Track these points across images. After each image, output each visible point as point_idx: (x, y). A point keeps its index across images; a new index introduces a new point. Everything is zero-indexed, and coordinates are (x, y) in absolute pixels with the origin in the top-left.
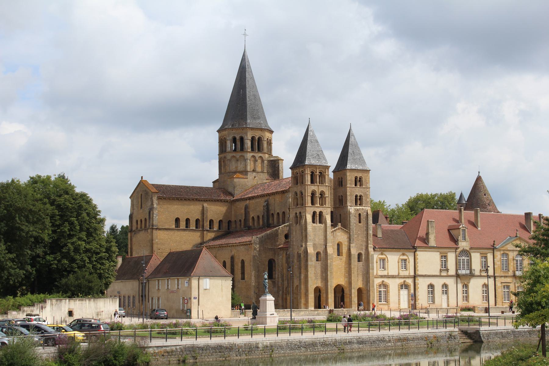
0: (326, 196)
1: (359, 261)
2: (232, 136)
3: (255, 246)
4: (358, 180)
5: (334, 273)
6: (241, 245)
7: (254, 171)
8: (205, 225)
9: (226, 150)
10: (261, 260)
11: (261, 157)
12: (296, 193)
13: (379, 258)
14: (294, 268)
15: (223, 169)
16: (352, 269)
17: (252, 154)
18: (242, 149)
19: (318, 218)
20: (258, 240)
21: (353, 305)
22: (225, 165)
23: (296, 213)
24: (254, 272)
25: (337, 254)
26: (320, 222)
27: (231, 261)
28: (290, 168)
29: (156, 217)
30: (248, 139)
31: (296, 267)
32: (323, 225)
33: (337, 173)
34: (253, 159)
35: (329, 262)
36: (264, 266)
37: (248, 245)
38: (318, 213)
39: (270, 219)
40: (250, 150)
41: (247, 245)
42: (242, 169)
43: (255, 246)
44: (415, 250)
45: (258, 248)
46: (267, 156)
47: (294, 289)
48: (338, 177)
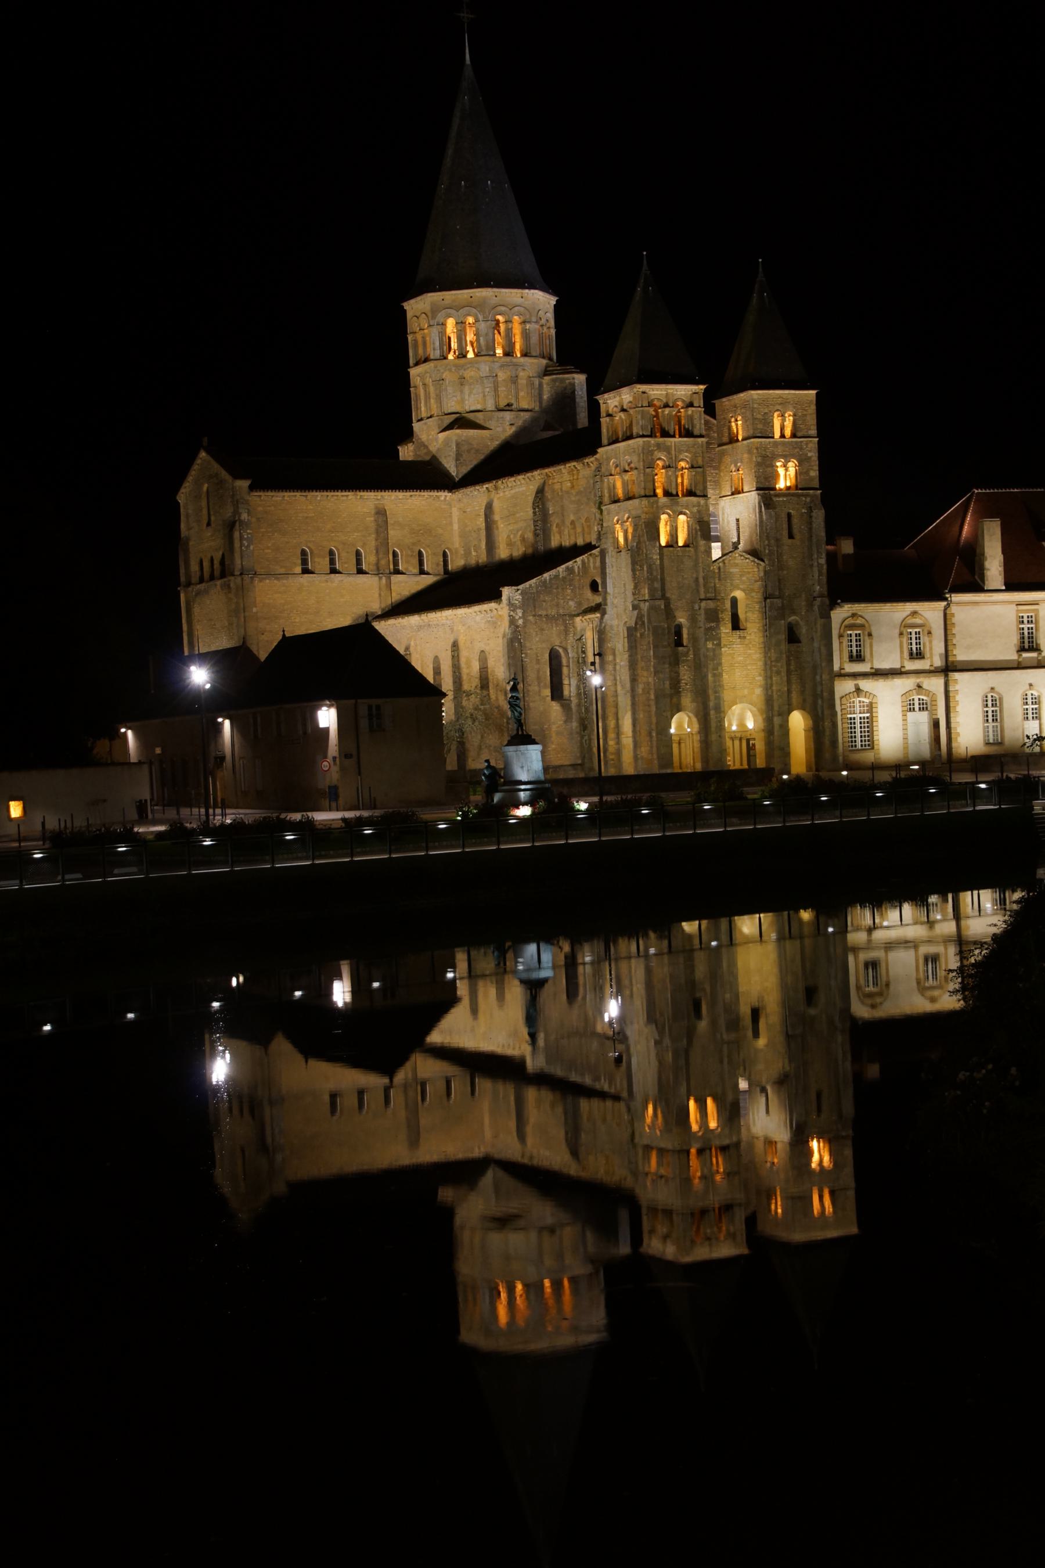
3: (512, 613)
8: (383, 562)
14: (618, 667)
15: (423, 409)
25: (730, 625)
27: (453, 656)
29: (248, 546)
31: (622, 663)
43: (512, 613)
44: (945, 603)
45: (520, 618)
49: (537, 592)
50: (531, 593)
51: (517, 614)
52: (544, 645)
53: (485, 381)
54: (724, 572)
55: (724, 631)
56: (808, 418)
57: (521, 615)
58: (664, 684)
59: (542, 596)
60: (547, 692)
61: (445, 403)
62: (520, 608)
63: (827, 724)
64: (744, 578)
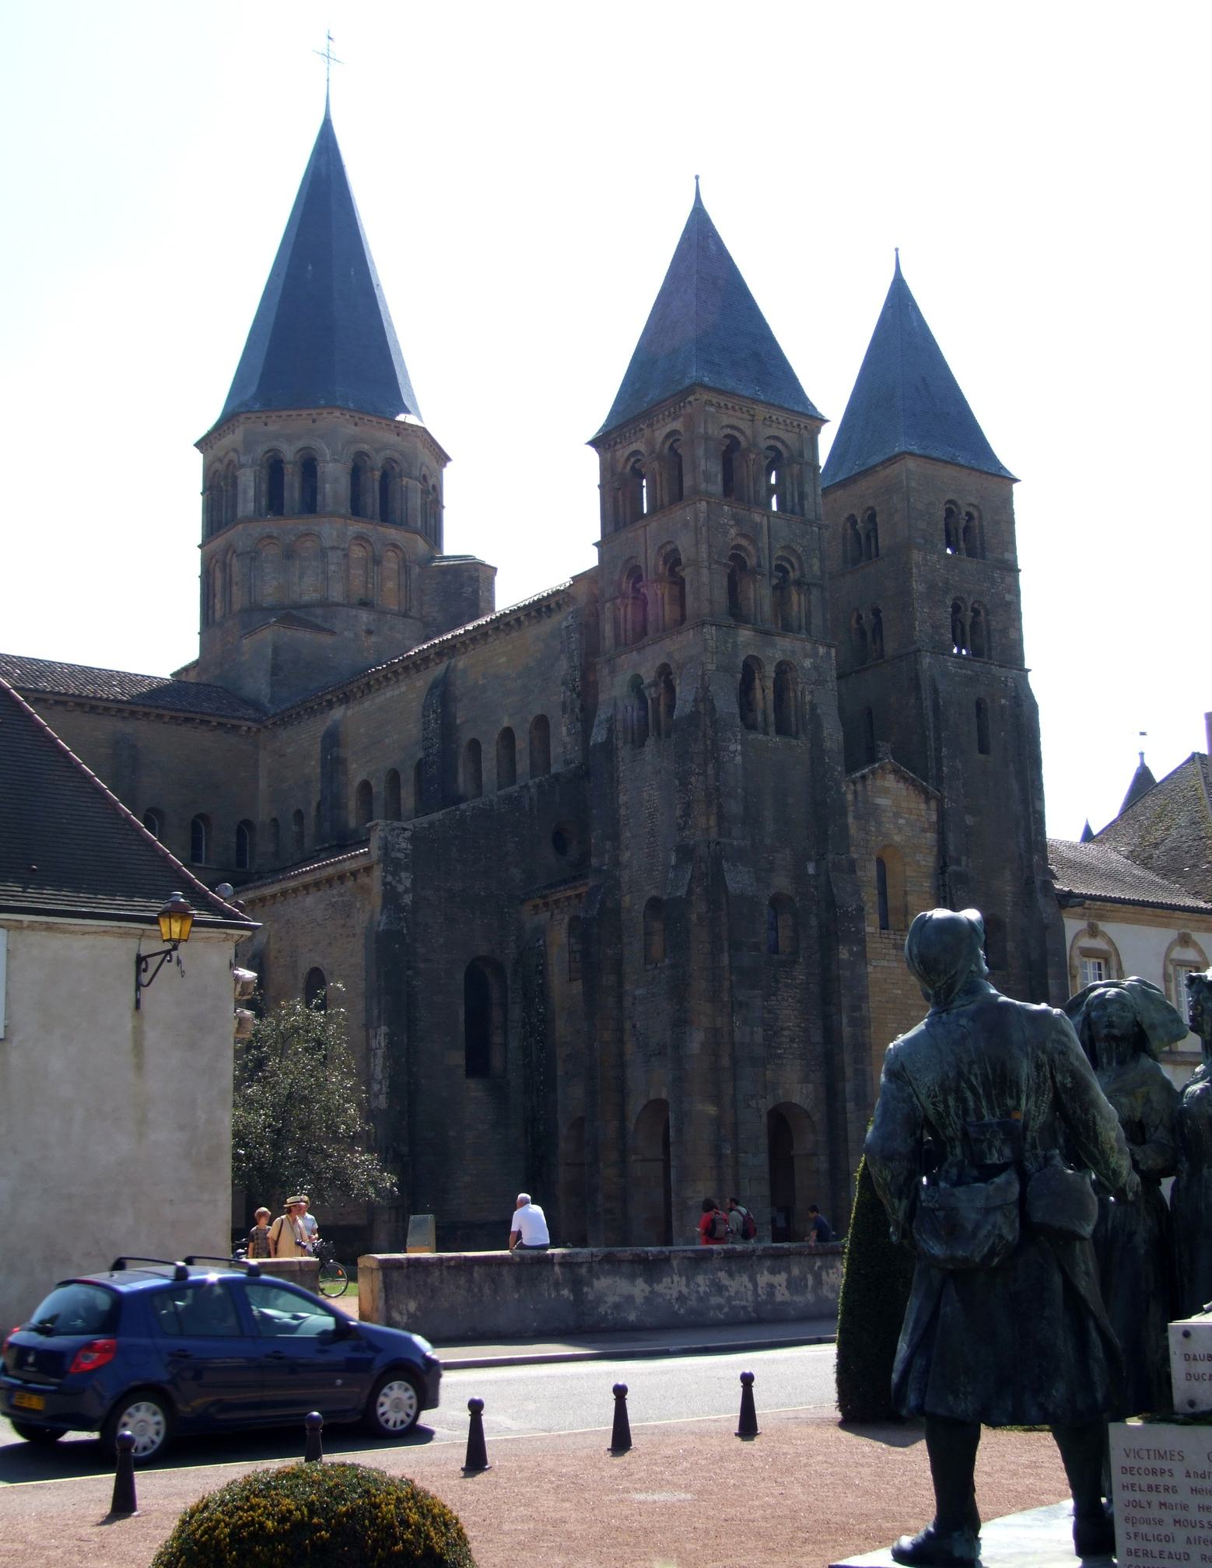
2: (265, 447)
3: (389, 878)
4: (963, 523)
6: (306, 887)
7: (364, 604)
9: (235, 514)
11: (395, 546)
12: (635, 574)
15: (218, 607)
17: (356, 527)
18: (310, 505)
19: (770, 695)
22: (228, 584)
23: (636, 684)
24: (384, 1029)
26: (782, 729)
28: (593, 443)
30: (336, 461)
32: (801, 744)
33: (840, 492)
34: (357, 552)
35: (844, 954)
37: (350, 883)
38: (770, 671)
39: (461, 770)
40: (345, 509)
41: (342, 878)
42: (306, 598)
43: (389, 878)
45: (406, 891)
46: (421, 546)
47: (631, 1126)
48: (846, 515)
51: (400, 881)
53: (330, 553)
57: (408, 885)
60: (458, 1058)
64: (901, 821)
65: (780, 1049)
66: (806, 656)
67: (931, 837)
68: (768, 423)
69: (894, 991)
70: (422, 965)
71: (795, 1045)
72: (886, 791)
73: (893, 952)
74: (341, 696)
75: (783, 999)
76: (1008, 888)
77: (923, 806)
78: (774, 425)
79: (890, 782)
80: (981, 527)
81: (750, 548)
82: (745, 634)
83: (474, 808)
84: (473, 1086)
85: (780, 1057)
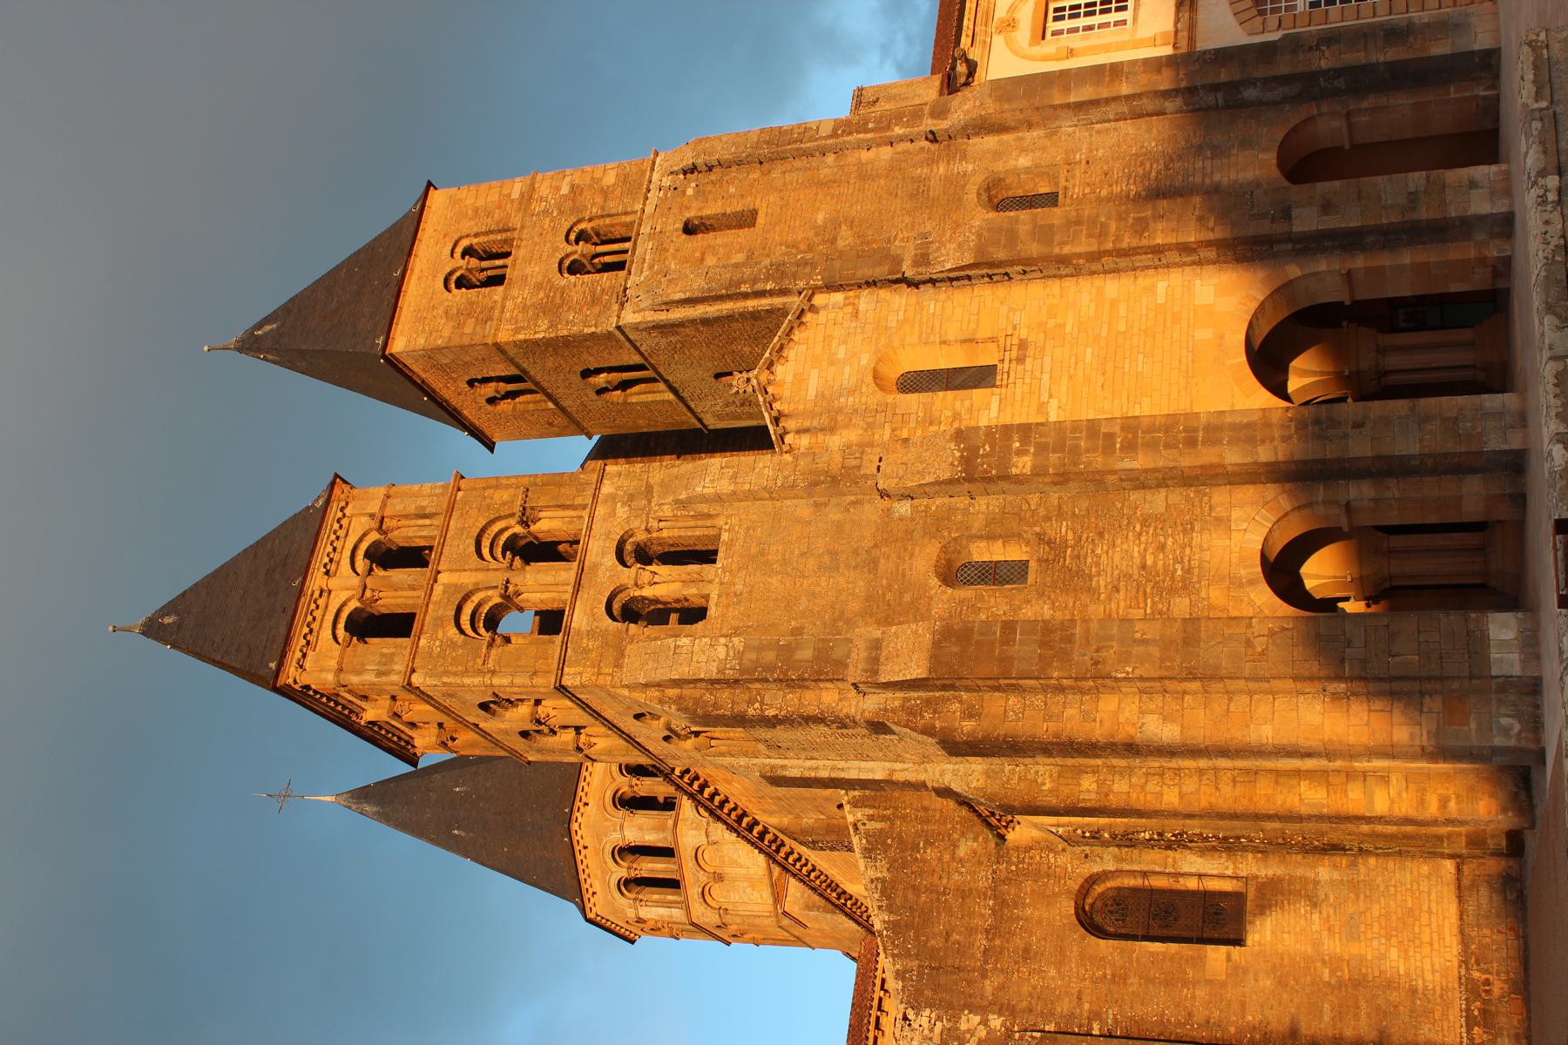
0: (517, 509)
1: (1051, 199)
2: (617, 894)
4: (474, 262)
5: (1145, 408)
10: (1079, 999)
13: (1031, 45)
16: (1109, 246)
18: (667, 853)
20: (923, 1019)
21: (1453, 213)
25: (978, 394)
30: (622, 828)
32: (730, 529)
36: (1133, 980)
38: (627, 575)
45: (984, 1022)
49: (917, 956)
50: (921, 975)
51: (972, 1032)
52: (1073, 952)
53: (713, 838)
54: (812, 414)
55: (994, 413)
56: (481, 203)
57: (977, 1019)
58: (1143, 642)
59: (932, 942)
60: (1216, 955)
61: (756, 908)
62: (955, 1018)
63: (1325, 61)
64: (841, 352)
65: (1176, 570)
66: (613, 514)
67: (866, 300)
68: (333, 567)
69: (1088, 360)
70: (1087, 1006)
71: (1170, 541)
72: (800, 379)
73: (1028, 361)
74: (829, 891)
75: (1098, 564)
76: (941, 169)
77: (822, 317)
78: (336, 557)
79: (784, 372)
80: (476, 235)
81: (476, 598)
82: (579, 620)
83: (880, 908)
84: (1257, 937)
85: (1189, 571)
